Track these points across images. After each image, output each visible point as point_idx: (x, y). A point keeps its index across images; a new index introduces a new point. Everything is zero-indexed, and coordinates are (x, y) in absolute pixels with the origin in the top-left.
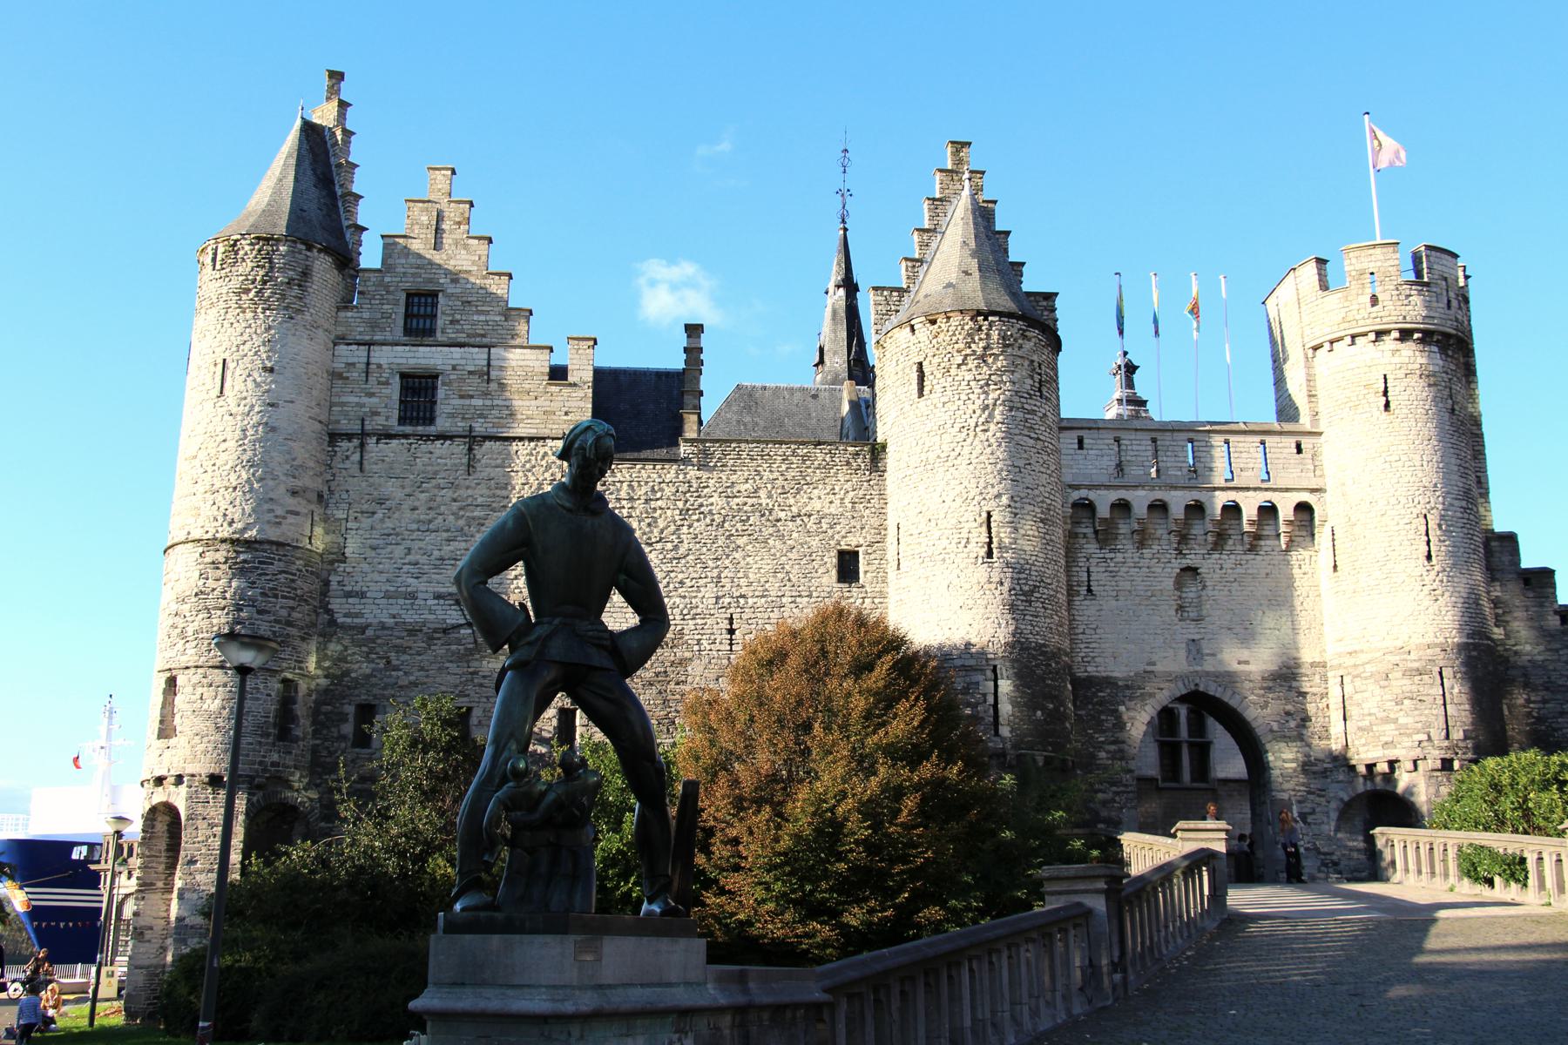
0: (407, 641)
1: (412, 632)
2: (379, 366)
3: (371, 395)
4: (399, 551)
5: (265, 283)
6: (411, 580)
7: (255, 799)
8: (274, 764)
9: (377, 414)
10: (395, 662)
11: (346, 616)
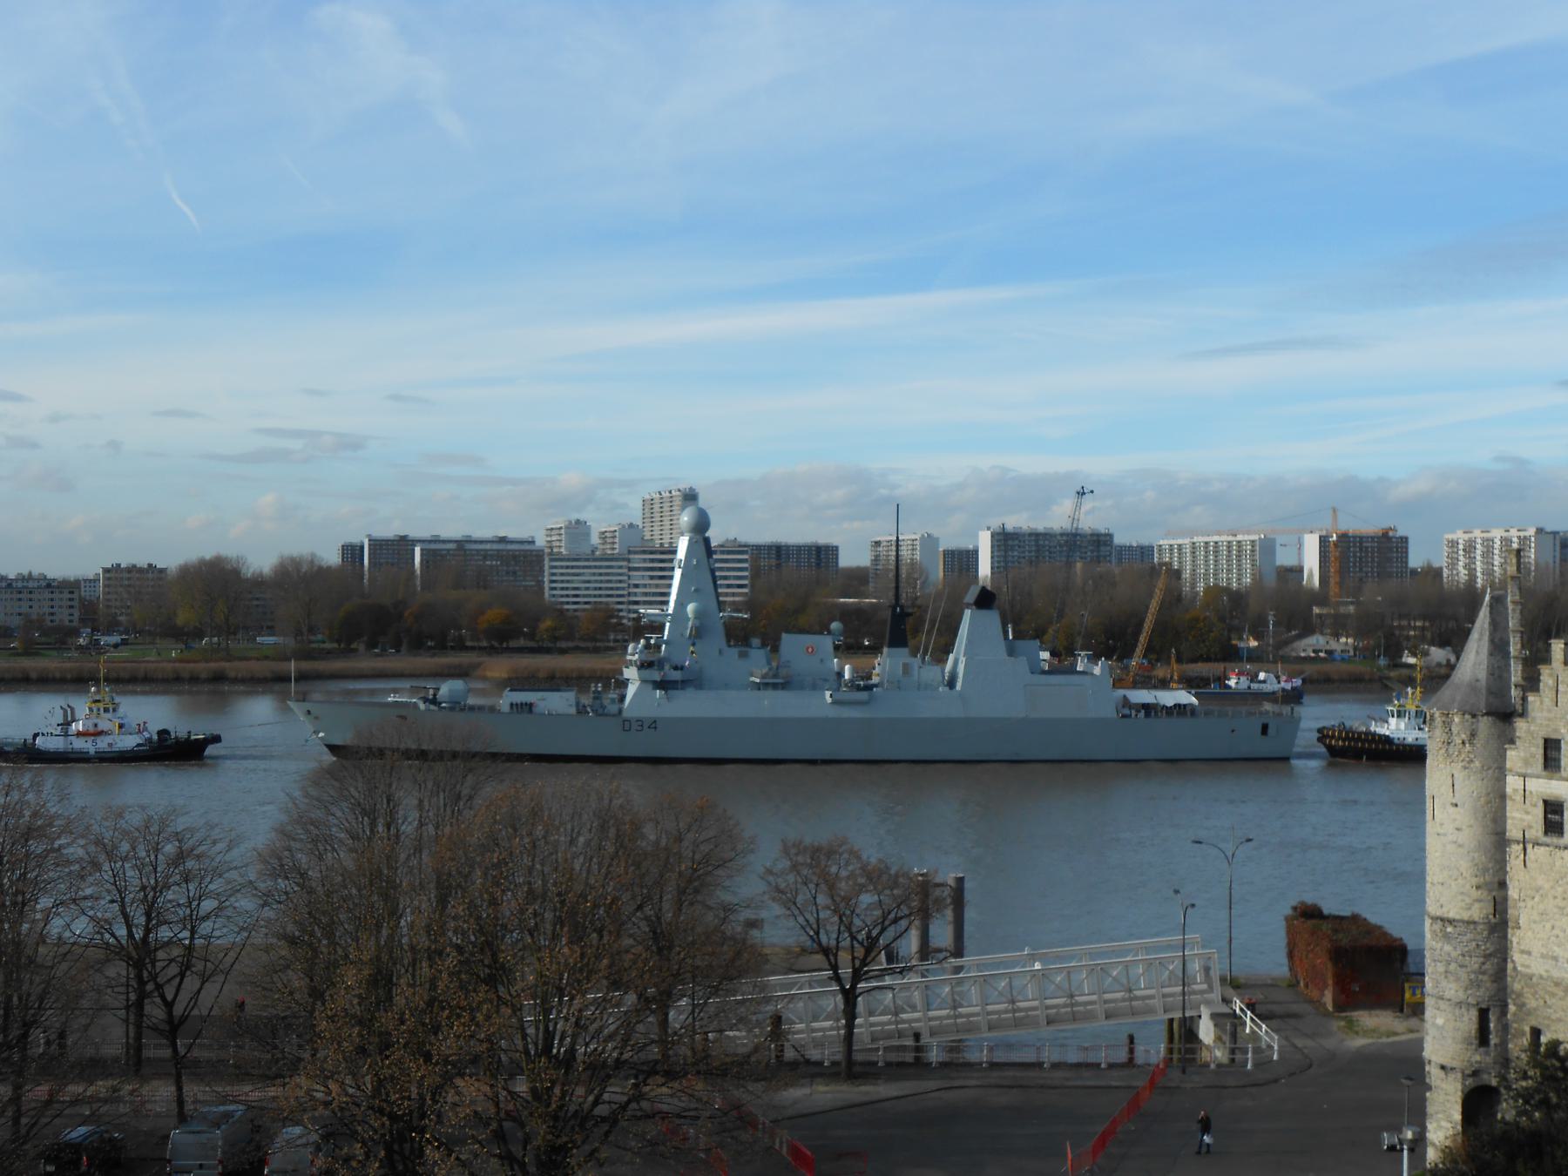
0: (1555, 990)
1: (1557, 984)
2: (1531, 792)
3: (1527, 813)
4: (1548, 926)
5: (1449, 743)
6: (1556, 948)
7: (1467, 1083)
8: (1476, 1062)
9: (1530, 827)
10: (1548, 1002)
11: (1523, 965)
